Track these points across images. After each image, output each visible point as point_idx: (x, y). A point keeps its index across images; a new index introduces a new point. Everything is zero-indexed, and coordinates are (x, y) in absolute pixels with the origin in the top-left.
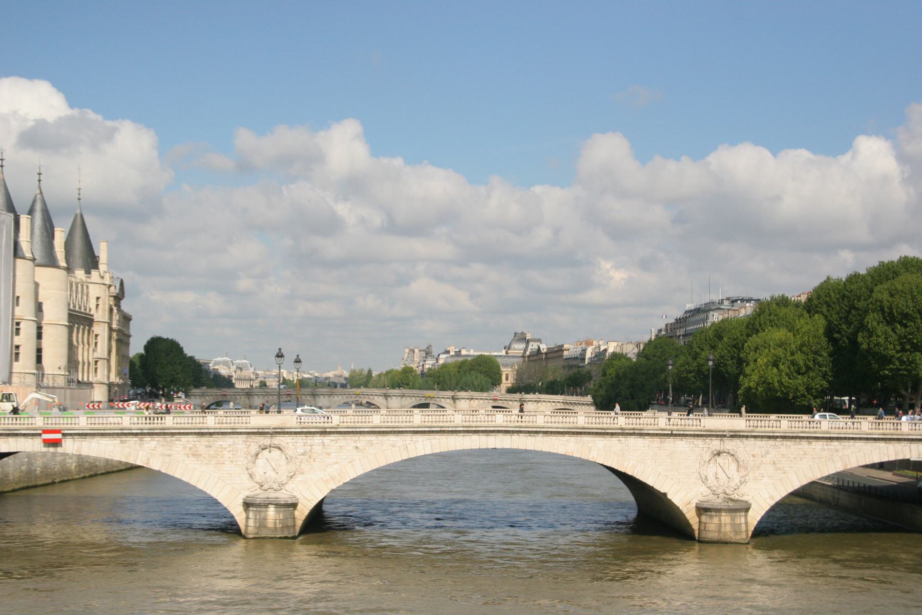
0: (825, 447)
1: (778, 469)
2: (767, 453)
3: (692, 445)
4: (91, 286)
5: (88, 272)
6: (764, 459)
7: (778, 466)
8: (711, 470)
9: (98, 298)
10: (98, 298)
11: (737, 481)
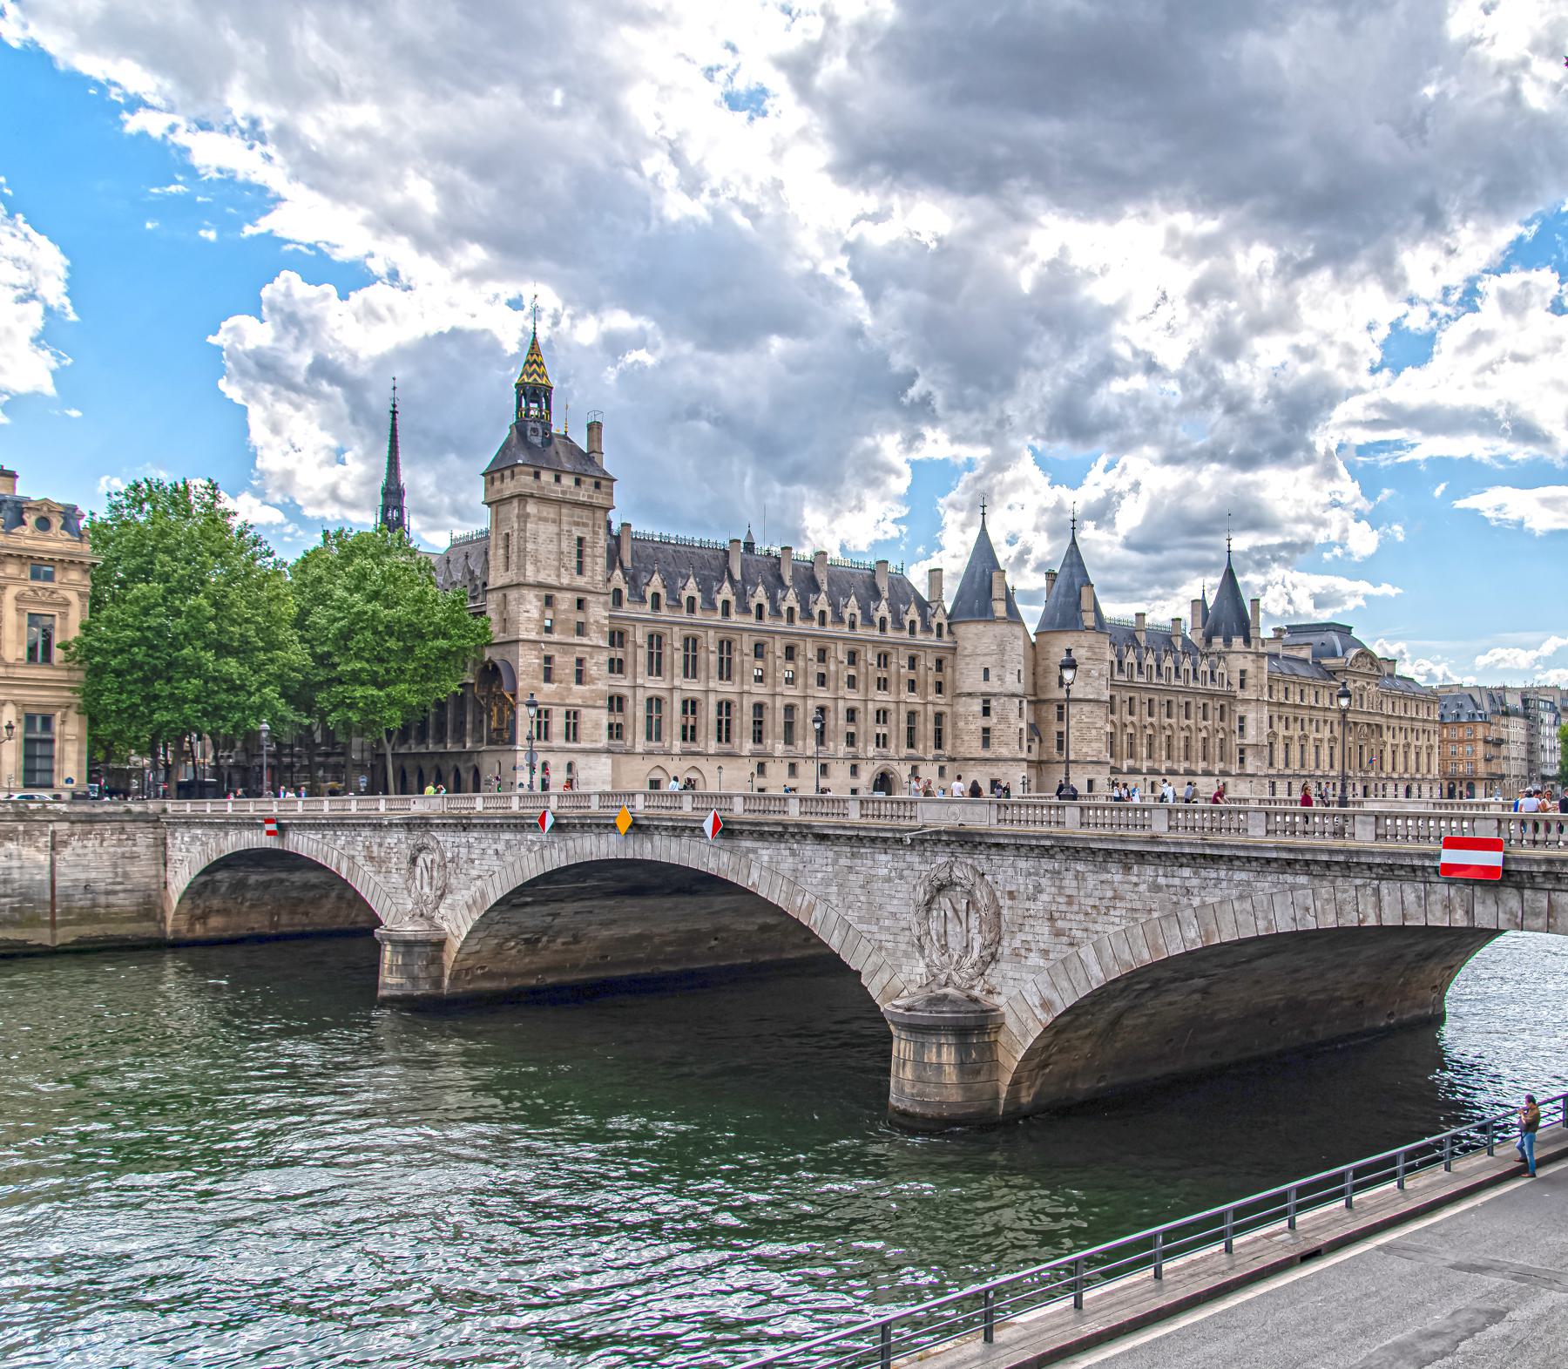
4: (1232, 656)
5: (1228, 642)
9: (1243, 672)
10: (1243, 672)
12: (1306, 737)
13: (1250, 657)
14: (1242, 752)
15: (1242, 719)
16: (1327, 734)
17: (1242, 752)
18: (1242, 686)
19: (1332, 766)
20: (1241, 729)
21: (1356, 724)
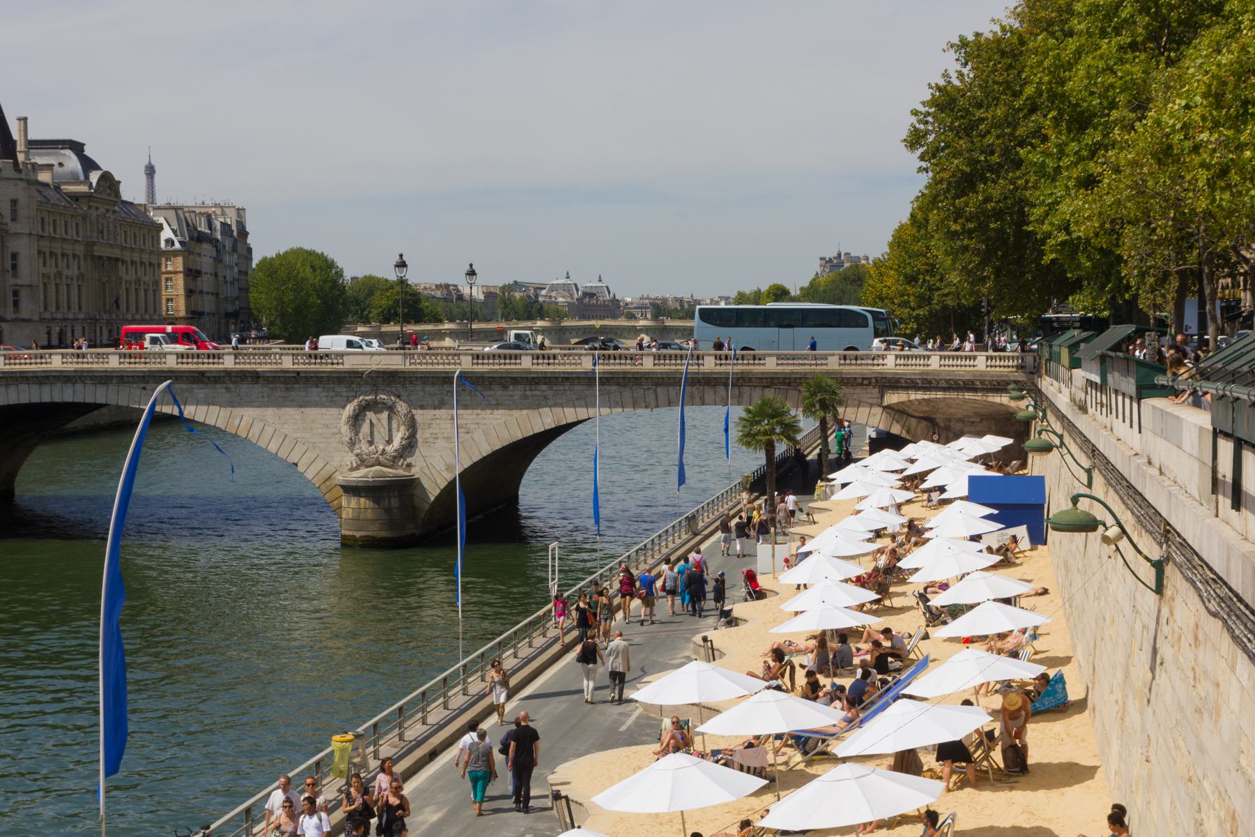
0: (528, 393)
3: (331, 394)
10: (14, 202)
11: (396, 443)
12: (59, 274)
13: (22, 185)
14: (16, 293)
15: (14, 256)
16: (76, 272)
17: (16, 293)
18: (13, 220)
19: (80, 308)
20: (14, 267)
21: (100, 258)
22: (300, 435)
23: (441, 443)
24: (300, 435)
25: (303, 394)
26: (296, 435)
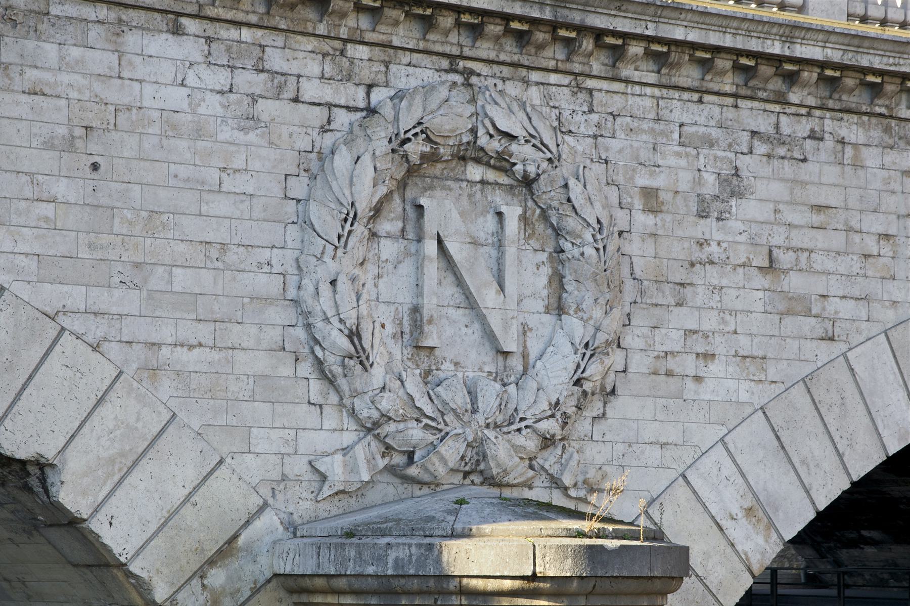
1: (797, 306)
2: (733, 185)
3: (249, 81)
6: (708, 227)
7: (795, 283)
8: (382, 286)
11: (555, 374)
22: (75, 297)
23: (723, 382)
24: (75, 297)
25: (101, 60)
26: (50, 296)
